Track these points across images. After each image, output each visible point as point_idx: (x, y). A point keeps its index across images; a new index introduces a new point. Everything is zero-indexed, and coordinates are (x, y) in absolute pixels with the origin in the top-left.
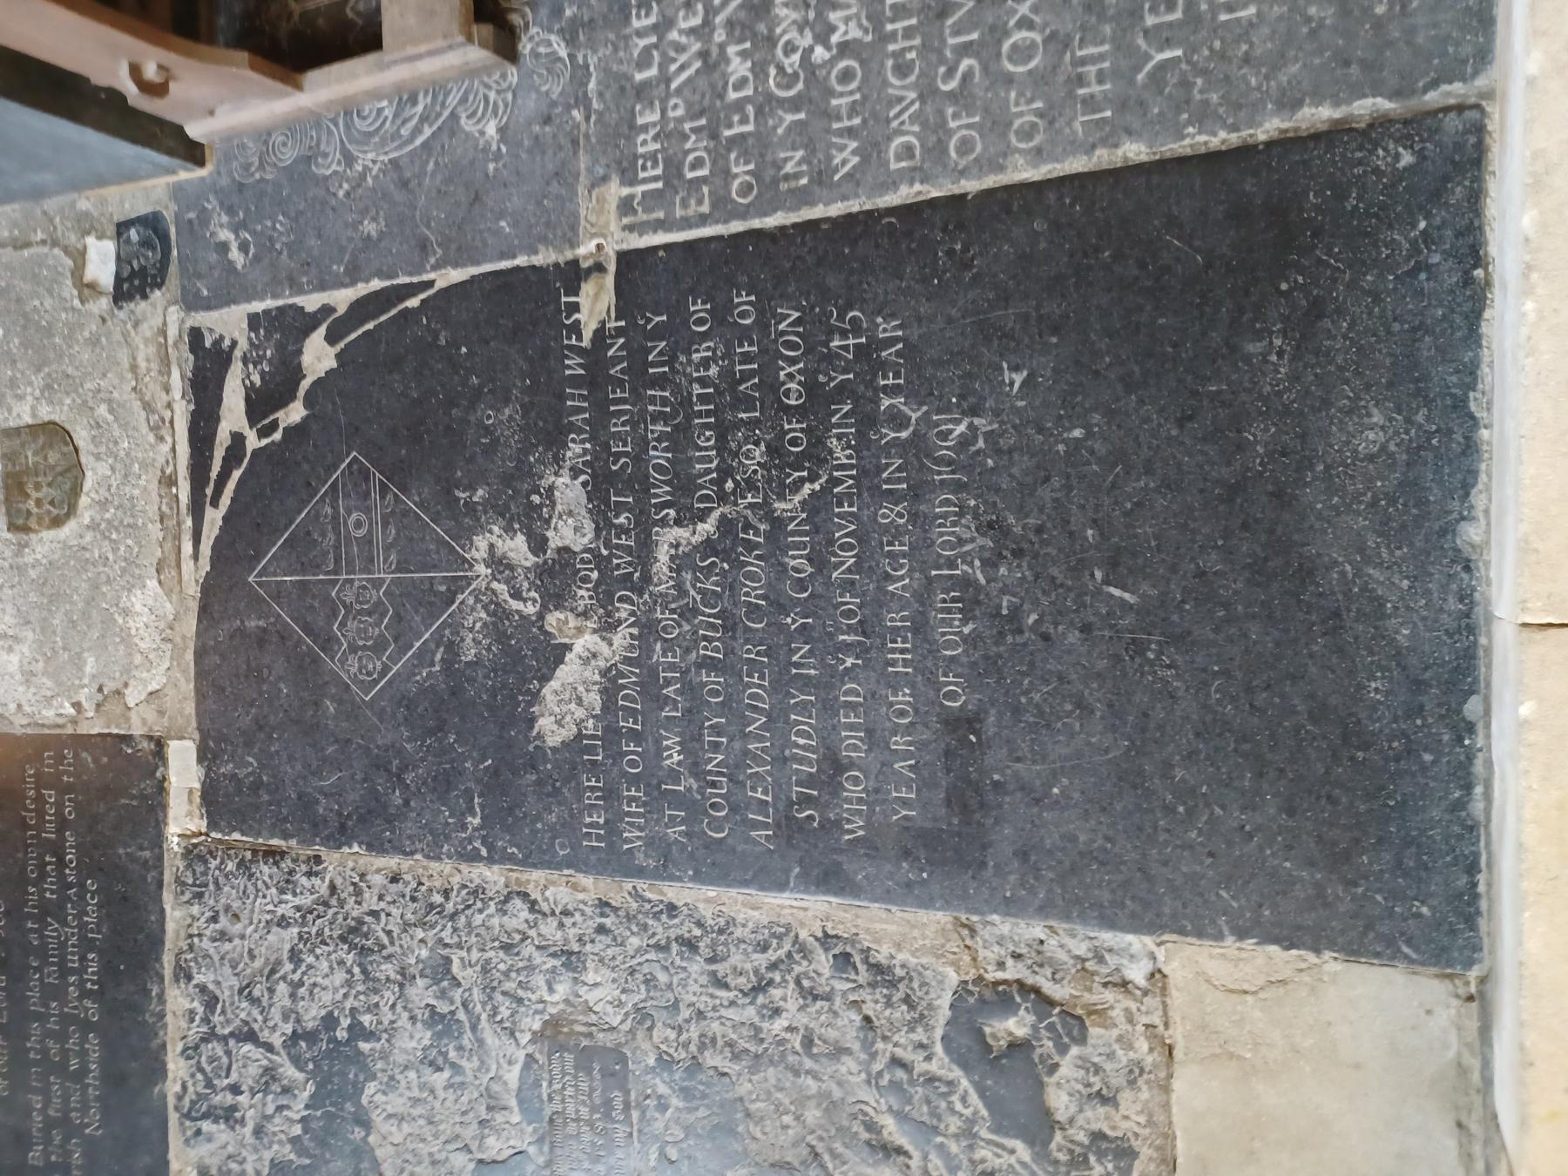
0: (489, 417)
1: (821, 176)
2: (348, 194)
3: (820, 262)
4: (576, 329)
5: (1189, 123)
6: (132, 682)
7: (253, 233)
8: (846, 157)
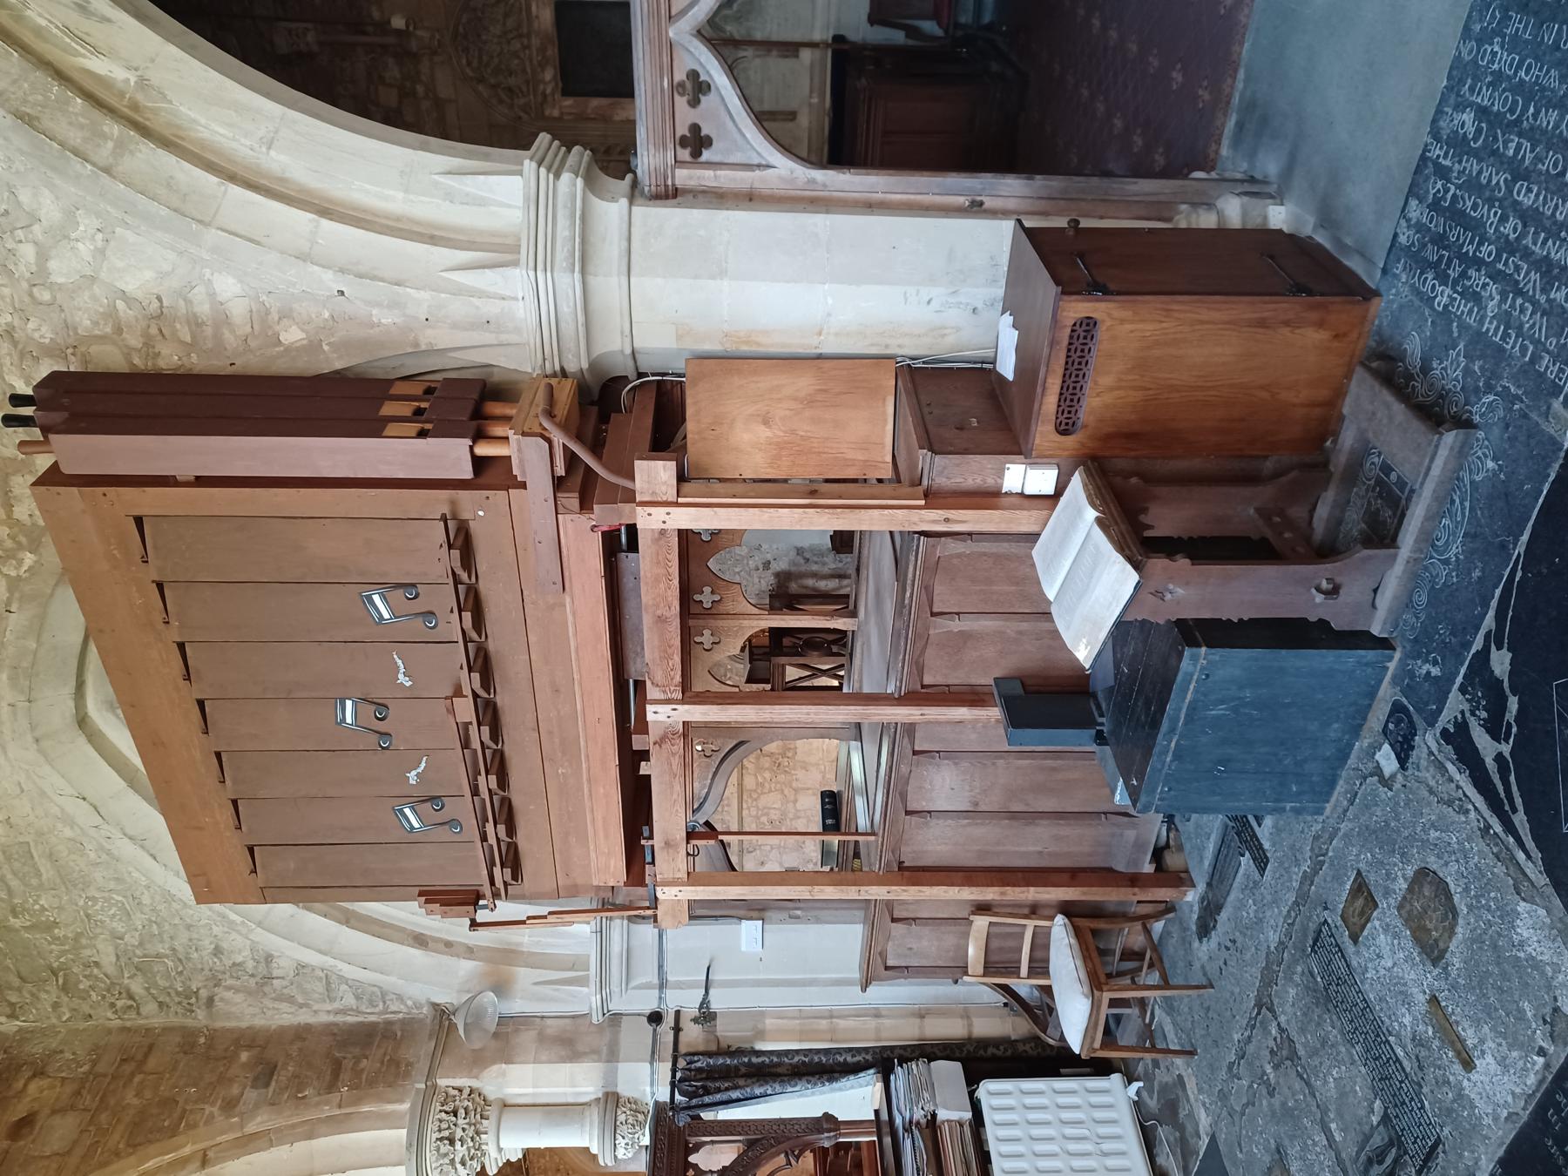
6: (1558, 992)
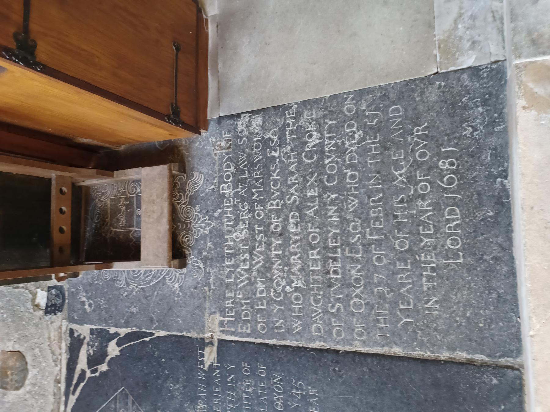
0: (171, 387)
1: (289, 331)
2: (127, 296)
3: (288, 361)
4: (202, 362)
5: (416, 346)
7: (94, 301)
8: (297, 325)
